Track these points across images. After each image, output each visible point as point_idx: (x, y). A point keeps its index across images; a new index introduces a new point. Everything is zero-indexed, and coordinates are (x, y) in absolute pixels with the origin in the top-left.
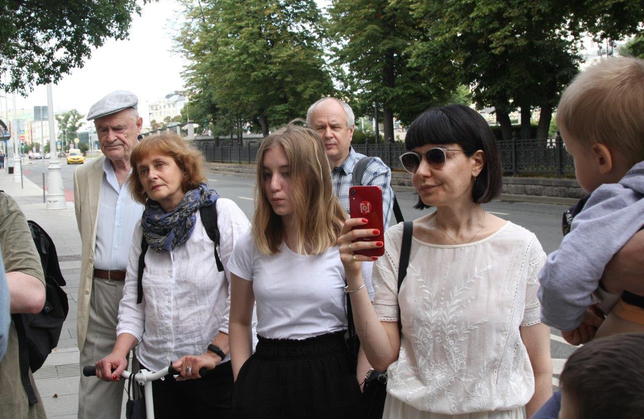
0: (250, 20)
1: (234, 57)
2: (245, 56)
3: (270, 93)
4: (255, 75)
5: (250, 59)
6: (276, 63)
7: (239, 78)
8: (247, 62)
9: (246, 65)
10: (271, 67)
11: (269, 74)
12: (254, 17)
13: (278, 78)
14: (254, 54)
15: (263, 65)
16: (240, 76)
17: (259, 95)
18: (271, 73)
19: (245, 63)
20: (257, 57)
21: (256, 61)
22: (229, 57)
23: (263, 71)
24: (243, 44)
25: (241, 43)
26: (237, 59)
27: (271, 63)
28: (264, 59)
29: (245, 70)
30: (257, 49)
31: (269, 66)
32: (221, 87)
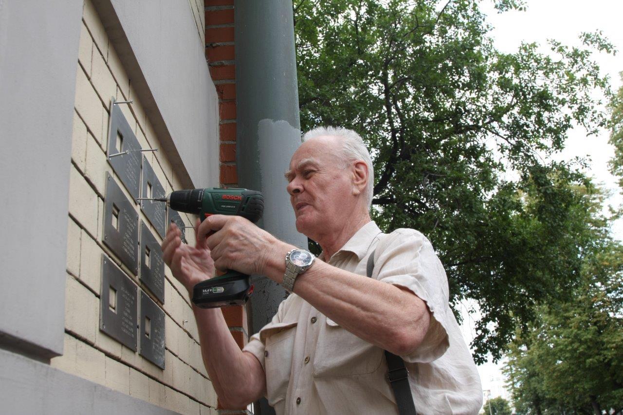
0: (575, 310)
1: (566, 346)
2: (576, 345)
3: (607, 379)
4: (591, 362)
5: (583, 346)
6: (611, 348)
7: (572, 367)
8: (581, 350)
9: (580, 353)
10: (605, 352)
11: (604, 360)
12: (579, 307)
13: (613, 364)
14: (586, 342)
15: (596, 351)
16: (573, 364)
17: (594, 382)
18: (606, 358)
19: (578, 351)
20: (589, 344)
21: (589, 348)
22: (562, 347)
23: (597, 357)
24: (574, 333)
25: (572, 331)
26: (570, 348)
27: (606, 349)
28: (597, 345)
29: (579, 357)
30: (590, 336)
31: (602, 352)
32: (550, 377)
